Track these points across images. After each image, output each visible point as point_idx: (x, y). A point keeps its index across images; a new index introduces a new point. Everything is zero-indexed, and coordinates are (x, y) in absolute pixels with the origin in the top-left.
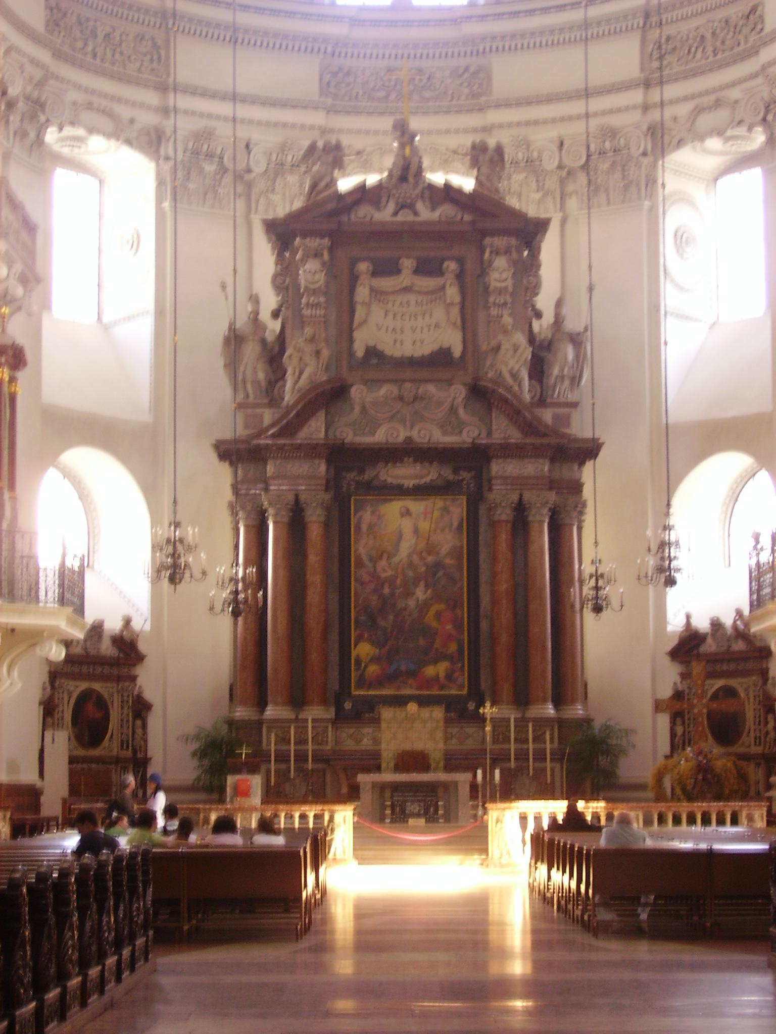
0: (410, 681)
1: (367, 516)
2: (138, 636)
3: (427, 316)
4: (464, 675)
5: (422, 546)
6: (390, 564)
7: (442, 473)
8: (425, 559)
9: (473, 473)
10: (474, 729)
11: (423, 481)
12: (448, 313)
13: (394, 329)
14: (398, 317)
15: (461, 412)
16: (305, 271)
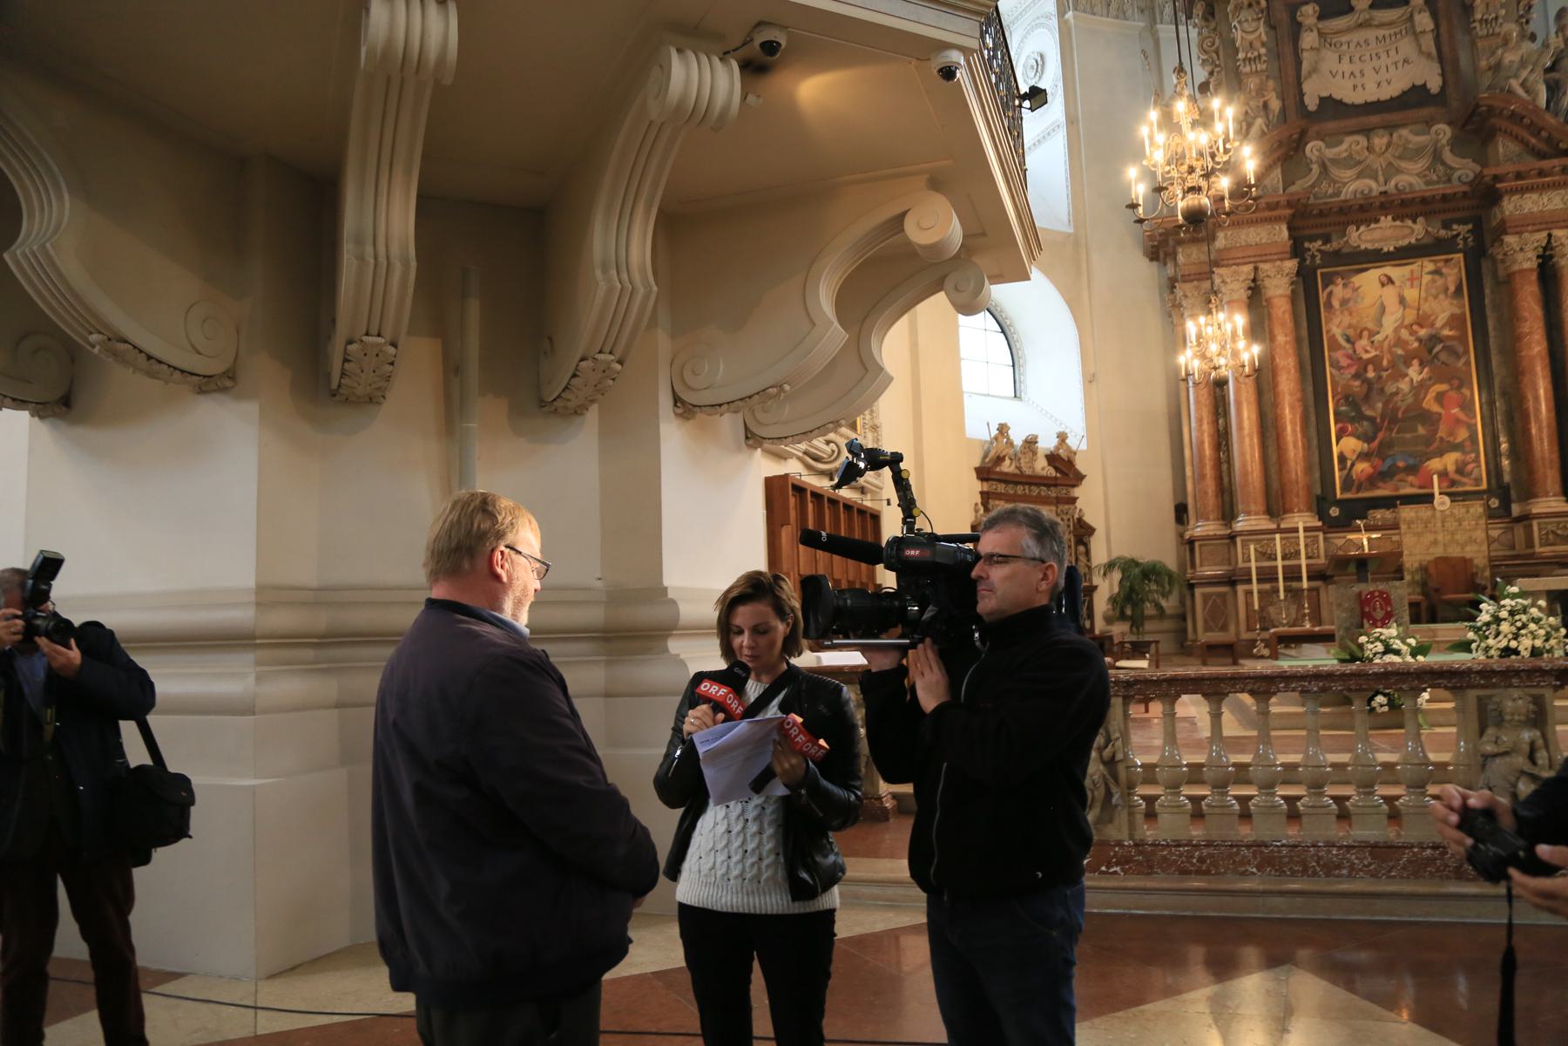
0: (1410, 478)
1: (1338, 291)
2: (1075, 453)
3: (1392, 53)
4: (1480, 466)
5: (1411, 316)
6: (1373, 342)
7: (1430, 229)
8: (1416, 332)
9: (1470, 226)
10: (1499, 532)
11: (1405, 242)
12: (1420, 46)
13: (1352, 73)
14: (1356, 59)
15: (1448, 156)
16: (1239, 22)
